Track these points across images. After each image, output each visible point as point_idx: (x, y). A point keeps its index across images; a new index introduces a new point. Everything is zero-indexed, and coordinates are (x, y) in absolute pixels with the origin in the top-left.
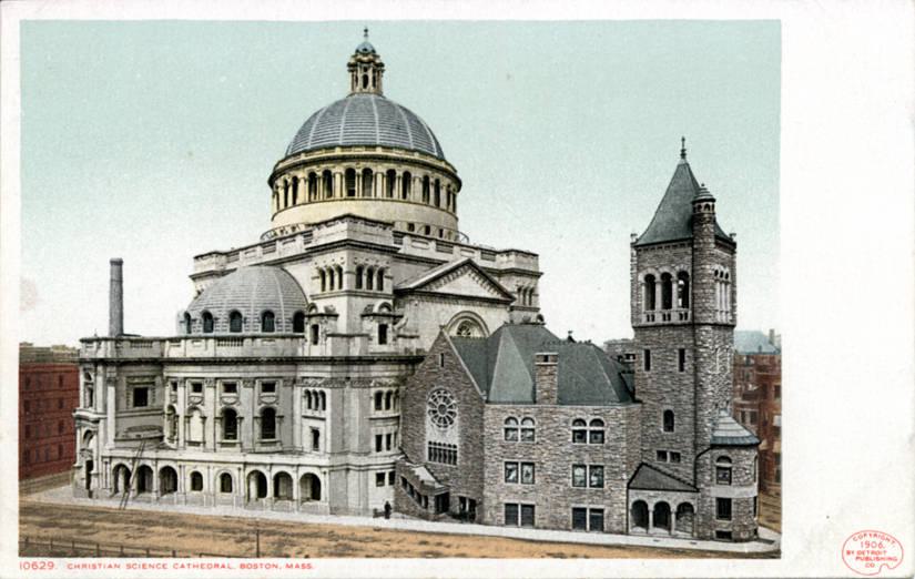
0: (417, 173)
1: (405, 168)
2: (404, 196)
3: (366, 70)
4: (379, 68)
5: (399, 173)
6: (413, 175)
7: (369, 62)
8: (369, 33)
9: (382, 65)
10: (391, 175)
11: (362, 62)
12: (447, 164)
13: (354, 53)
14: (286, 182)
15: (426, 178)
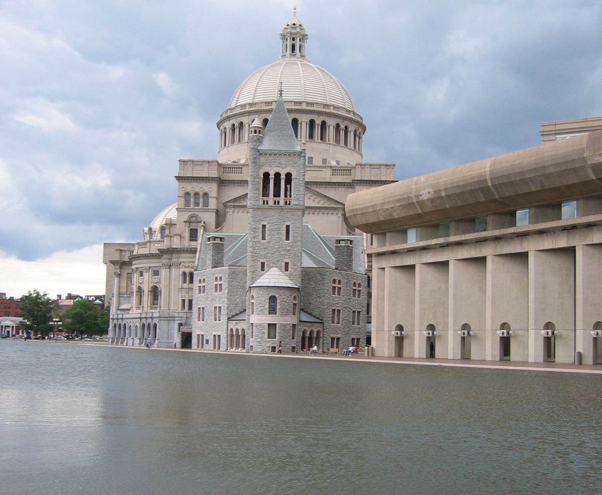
0: (331, 123)
1: (322, 118)
2: (322, 139)
3: (294, 39)
4: (304, 38)
5: (318, 121)
6: (328, 124)
7: (296, 34)
8: (296, 11)
9: (306, 35)
10: (312, 123)
11: (291, 34)
12: (354, 114)
13: (285, 26)
14: (234, 125)
15: (338, 125)
